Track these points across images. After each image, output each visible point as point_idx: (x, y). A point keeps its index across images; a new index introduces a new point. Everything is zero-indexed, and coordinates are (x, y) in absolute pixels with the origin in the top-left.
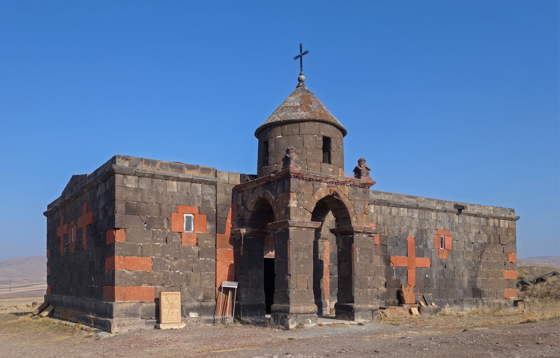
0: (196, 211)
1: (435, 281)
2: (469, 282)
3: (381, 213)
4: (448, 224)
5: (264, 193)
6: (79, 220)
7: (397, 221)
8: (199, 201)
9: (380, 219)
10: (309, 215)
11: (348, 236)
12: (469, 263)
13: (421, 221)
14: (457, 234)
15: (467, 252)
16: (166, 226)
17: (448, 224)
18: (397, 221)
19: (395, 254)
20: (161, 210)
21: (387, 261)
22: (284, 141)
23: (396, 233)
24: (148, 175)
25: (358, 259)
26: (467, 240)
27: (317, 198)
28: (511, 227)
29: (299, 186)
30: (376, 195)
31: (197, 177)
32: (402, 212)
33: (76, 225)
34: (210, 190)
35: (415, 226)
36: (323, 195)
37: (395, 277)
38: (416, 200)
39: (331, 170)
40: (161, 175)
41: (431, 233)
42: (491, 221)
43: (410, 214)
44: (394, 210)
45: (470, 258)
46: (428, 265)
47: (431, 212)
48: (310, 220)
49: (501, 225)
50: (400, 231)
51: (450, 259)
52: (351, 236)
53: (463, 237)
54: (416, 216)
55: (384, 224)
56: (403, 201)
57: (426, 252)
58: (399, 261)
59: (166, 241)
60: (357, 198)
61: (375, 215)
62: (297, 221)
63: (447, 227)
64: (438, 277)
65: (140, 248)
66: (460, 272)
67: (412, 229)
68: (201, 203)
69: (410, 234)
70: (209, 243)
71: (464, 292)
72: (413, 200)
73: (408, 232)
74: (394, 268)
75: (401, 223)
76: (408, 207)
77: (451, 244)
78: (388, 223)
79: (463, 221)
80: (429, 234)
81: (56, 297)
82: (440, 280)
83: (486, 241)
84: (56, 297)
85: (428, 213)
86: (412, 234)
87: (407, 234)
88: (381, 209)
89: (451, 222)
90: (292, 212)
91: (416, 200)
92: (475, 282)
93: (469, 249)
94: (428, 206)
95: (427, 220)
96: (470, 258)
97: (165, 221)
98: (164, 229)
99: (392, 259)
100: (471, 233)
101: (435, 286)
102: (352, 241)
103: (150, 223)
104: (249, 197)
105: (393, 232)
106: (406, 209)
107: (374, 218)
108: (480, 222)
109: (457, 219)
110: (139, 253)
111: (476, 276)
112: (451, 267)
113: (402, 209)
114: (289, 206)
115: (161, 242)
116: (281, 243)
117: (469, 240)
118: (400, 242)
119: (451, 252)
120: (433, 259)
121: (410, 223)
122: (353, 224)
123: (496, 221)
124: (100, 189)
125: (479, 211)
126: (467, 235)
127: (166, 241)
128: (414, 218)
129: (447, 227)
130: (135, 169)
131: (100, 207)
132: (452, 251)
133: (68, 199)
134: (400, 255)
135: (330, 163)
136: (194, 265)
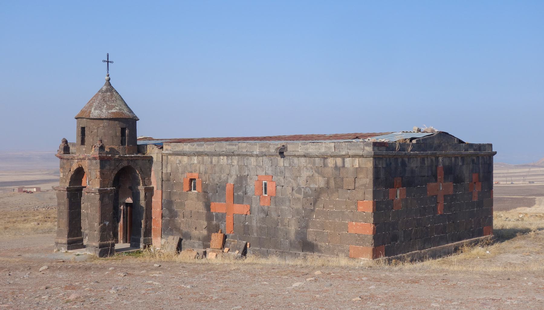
1: (255, 229)
2: (297, 233)
4: (270, 169)
9: (202, 169)
12: (298, 212)
13: (241, 168)
14: (282, 179)
15: (294, 199)
17: (270, 169)
18: (217, 169)
19: (215, 201)
21: (208, 207)
23: (216, 181)
28: (363, 166)
30: (200, 147)
32: (222, 161)
35: (234, 173)
37: (214, 222)
38: (237, 146)
39: (84, 149)
41: (251, 179)
42: (331, 162)
43: (230, 161)
44: (215, 159)
45: (299, 206)
47: (250, 158)
49: (347, 165)
50: (220, 179)
51: (273, 206)
53: (290, 182)
54: (235, 163)
55: (206, 173)
56: (224, 150)
57: (245, 199)
58: (217, 208)
61: (198, 165)
63: (270, 172)
64: (259, 225)
66: (286, 221)
67: (231, 177)
69: (229, 181)
71: (291, 244)
74: (214, 214)
75: (221, 171)
76: (227, 156)
77: (274, 190)
79: (290, 164)
80: (248, 180)
82: (261, 228)
85: (248, 159)
86: (231, 181)
87: (227, 182)
88: (203, 159)
89: (275, 165)
92: (305, 234)
93: (298, 196)
96: (299, 206)
99: (212, 205)
101: (255, 234)
105: (214, 180)
108: (314, 164)
109: (281, 161)
111: (307, 227)
112: (274, 215)
113: (222, 157)
118: (219, 189)
123: (339, 161)
126: (294, 179)
128: (233, 166)
132: (275, 197)
134: (219, 201)
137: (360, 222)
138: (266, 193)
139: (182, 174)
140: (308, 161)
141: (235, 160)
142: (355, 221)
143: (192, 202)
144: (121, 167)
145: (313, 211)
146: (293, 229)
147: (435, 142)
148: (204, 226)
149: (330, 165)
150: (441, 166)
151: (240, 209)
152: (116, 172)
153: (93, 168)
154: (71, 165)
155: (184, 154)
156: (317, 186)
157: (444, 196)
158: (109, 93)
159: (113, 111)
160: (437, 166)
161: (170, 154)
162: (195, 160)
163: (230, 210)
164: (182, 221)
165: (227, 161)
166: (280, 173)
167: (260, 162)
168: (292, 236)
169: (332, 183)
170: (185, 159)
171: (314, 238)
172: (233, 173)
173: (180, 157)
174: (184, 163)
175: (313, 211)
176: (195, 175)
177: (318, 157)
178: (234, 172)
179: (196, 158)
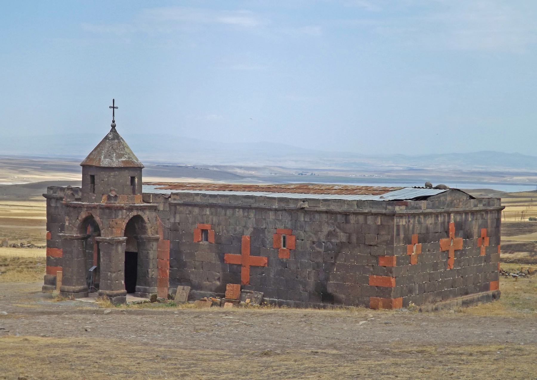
3: (216, 215)
7: (232, 221)
9: (215, 219)
12: (318, 265)
13: (257, 221)
14: (302, 233)
15: (315, 252)
17: (289, 223)
23: (231, 232)
32: (237, 213)
35: (251, 226)
41: (269, 232)
43: (246, 214)
44: (229, 212)
51: (292, 259)
53: (310, 236)
54: (252, 215)
55: (219, 224)
61: (211, 217)
67: (248, 229)
72: (251, 200)
73: (243, 231)
76: (244, 208)
79: (311, 219)
80: (266, 233)
87: (243, 234)
91: (254, 200)
93: (318, 249)
95: (265, 219)
96: (320, 260)
100: (321, 231)
106: (241, 210)
107: (210, 219)
111: (327, 279)
112: (293, 267)
113: (237, 210)
117: (319, 239)
119: (293, 251)
121: (246, 223)
123: (361, 218)
126: (315, 234)
128: (249, 218)
132: (295, 251)
135: (94, 193)
137: (381, 276)
138: (284, 246)
139: (192, 224)
140: (329, 217)
142: (376, 275)
143: (205, 252)
144: (131, 217)
145: (333, 264)
146: (312, 281)
147: (448, 199)
148: (216, 278)
149: (352, 222)
150: (452, 222)
152: (127, 221)
153: (105, 217)
154: (79, 213)
155: (195, 205)
156: (338, 241)
157: (455, 251)
158: (116, 141)
159: (123, 159)
160: (449, 222)
161: (179, 204)
162: (208, 211)
164: (193, 272)
165: (243, 214)
166: (300, 228)
167: (279, 215)
168: (311, 287)
169: (354, 239)
170: (196, 210)
171: (335, 290)
173: (190, 208)
174: (194, 213)
175: (333, 264)
176: (207, 226)
177: (340, 213)
178: (251, 224)
179: (208, 210)
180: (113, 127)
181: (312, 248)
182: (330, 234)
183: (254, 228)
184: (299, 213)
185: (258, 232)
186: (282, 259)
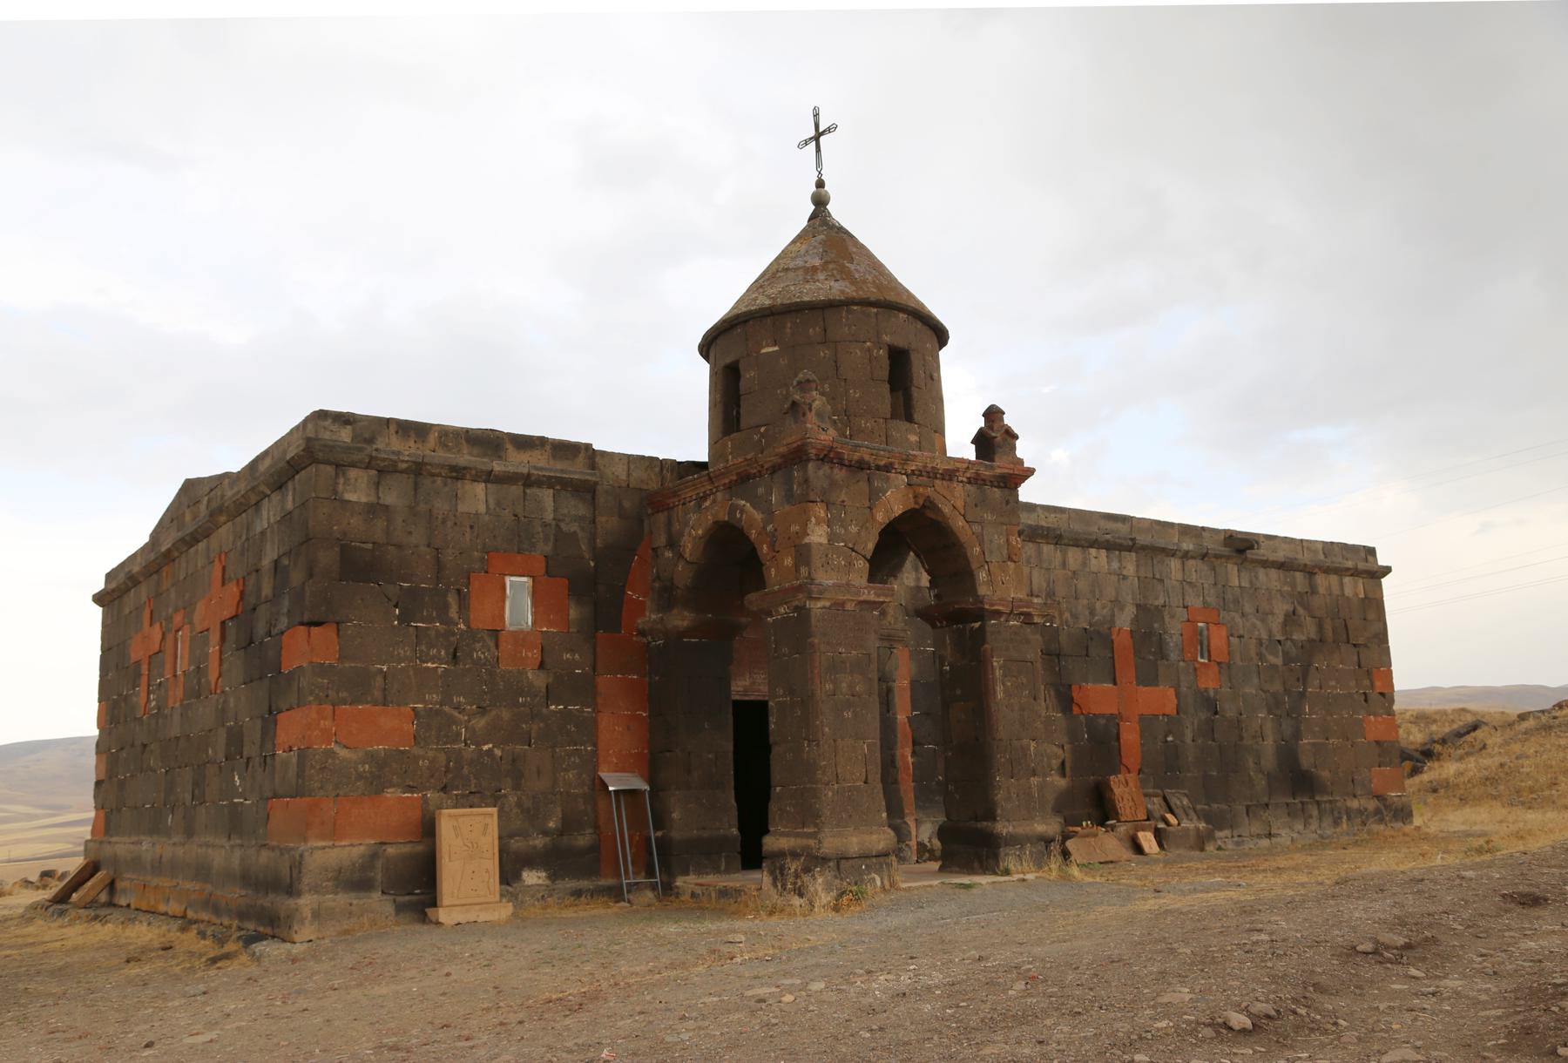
0: (540, 567)
5: (733, 509)
6: (200, 608)
7: (1082, 584)
8: (546, 540)
10: (862, 565)
11: (969, 626)
14: (1238, 619)
16: (453, 613)
20: (439, 565)
22: (783, 362)
24: (404, 466)
25: (999, 689)
26: (1264, 636)
27: (881, 518)
28: (1371, 595)
29: (833, 484)
31: (541, 469)
32: (1094, 561)
33: (191, 623)
34: (576, 507)
35: (1129, 599)
36: (898, 510)
40: (443, 466)
41: (1172, 617)
43: (1115, 565)
44: (1074, 556)
46: (1171, 709)
48: (864, 581)
49: (1348, 592)
52: (977, 625)
53: (1254, 626)
54: (1130, 570)
59: (455, 656)
60: (988, 517)
62: (830, 582)
63: (1212, 600)
65: (379, 679)
67: (1122, 608)
68: (551, 544)
69: (1118, 623)
70: (574, 659)
72: (1119, 525)
73: (1113, 615)
75: (1093, 592)
78: (1061, 592)
80: (1167, 619)
81: (122, 846)
83: (1313, 635)
84: (122, 846)
86: (1124, 620)
87: (1112, 622)
88: (1040, 553)
90: (817, 560)
93: (1272, 659)
94: (1161, 543)
97: (452, 600)
98: (448, 622)
102: (980, 636)
103: (410, 604)
104: (686, 524)
105: (1075, 616)
106: (1103, 552)
108: (1293, 585)
110: (377, 694)
113: (1093, 551)
114: (806, 540)
115: (441, 661)
116: (785, 650)
118: (1096, 641)
120: (1184, 689)
122: (982, 590)
123: (1334, 578)
124: (265, 513)
125: (1291, 555)
126: (1263, 621)
127: (455, 656)
128: (1125, 578)
129: (1212, 600)
130: (369, 449)
131: (266, 563)
133: (169, 551)
136: (535, 727)
141: (1130, 564)
148: (1055, 763)
149: (1322, 590)
151: (1160, 699)
163: (1129, 702)
172: (1128, 599)
180: (820, 201)
181: (1261, 656)
182: (1291, 619)
183: (1138, 606)
184: (1230, 566)
185: (1148, 614)
186: (1206, 690)
